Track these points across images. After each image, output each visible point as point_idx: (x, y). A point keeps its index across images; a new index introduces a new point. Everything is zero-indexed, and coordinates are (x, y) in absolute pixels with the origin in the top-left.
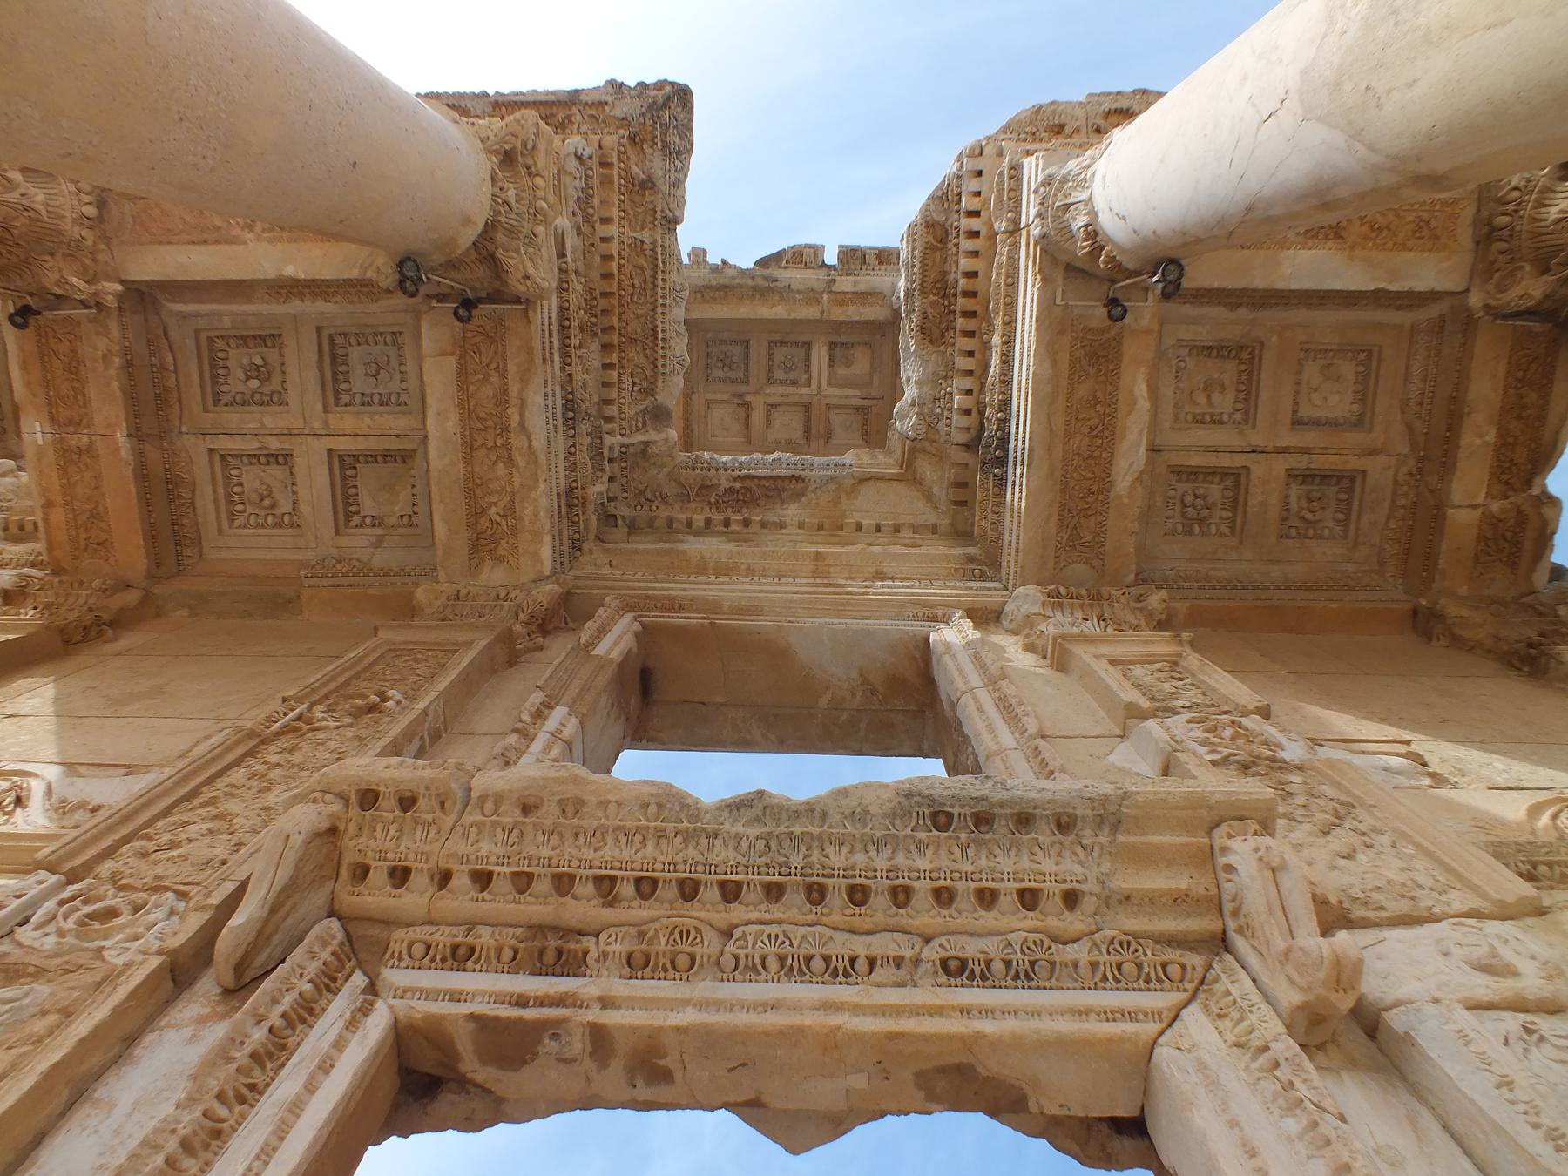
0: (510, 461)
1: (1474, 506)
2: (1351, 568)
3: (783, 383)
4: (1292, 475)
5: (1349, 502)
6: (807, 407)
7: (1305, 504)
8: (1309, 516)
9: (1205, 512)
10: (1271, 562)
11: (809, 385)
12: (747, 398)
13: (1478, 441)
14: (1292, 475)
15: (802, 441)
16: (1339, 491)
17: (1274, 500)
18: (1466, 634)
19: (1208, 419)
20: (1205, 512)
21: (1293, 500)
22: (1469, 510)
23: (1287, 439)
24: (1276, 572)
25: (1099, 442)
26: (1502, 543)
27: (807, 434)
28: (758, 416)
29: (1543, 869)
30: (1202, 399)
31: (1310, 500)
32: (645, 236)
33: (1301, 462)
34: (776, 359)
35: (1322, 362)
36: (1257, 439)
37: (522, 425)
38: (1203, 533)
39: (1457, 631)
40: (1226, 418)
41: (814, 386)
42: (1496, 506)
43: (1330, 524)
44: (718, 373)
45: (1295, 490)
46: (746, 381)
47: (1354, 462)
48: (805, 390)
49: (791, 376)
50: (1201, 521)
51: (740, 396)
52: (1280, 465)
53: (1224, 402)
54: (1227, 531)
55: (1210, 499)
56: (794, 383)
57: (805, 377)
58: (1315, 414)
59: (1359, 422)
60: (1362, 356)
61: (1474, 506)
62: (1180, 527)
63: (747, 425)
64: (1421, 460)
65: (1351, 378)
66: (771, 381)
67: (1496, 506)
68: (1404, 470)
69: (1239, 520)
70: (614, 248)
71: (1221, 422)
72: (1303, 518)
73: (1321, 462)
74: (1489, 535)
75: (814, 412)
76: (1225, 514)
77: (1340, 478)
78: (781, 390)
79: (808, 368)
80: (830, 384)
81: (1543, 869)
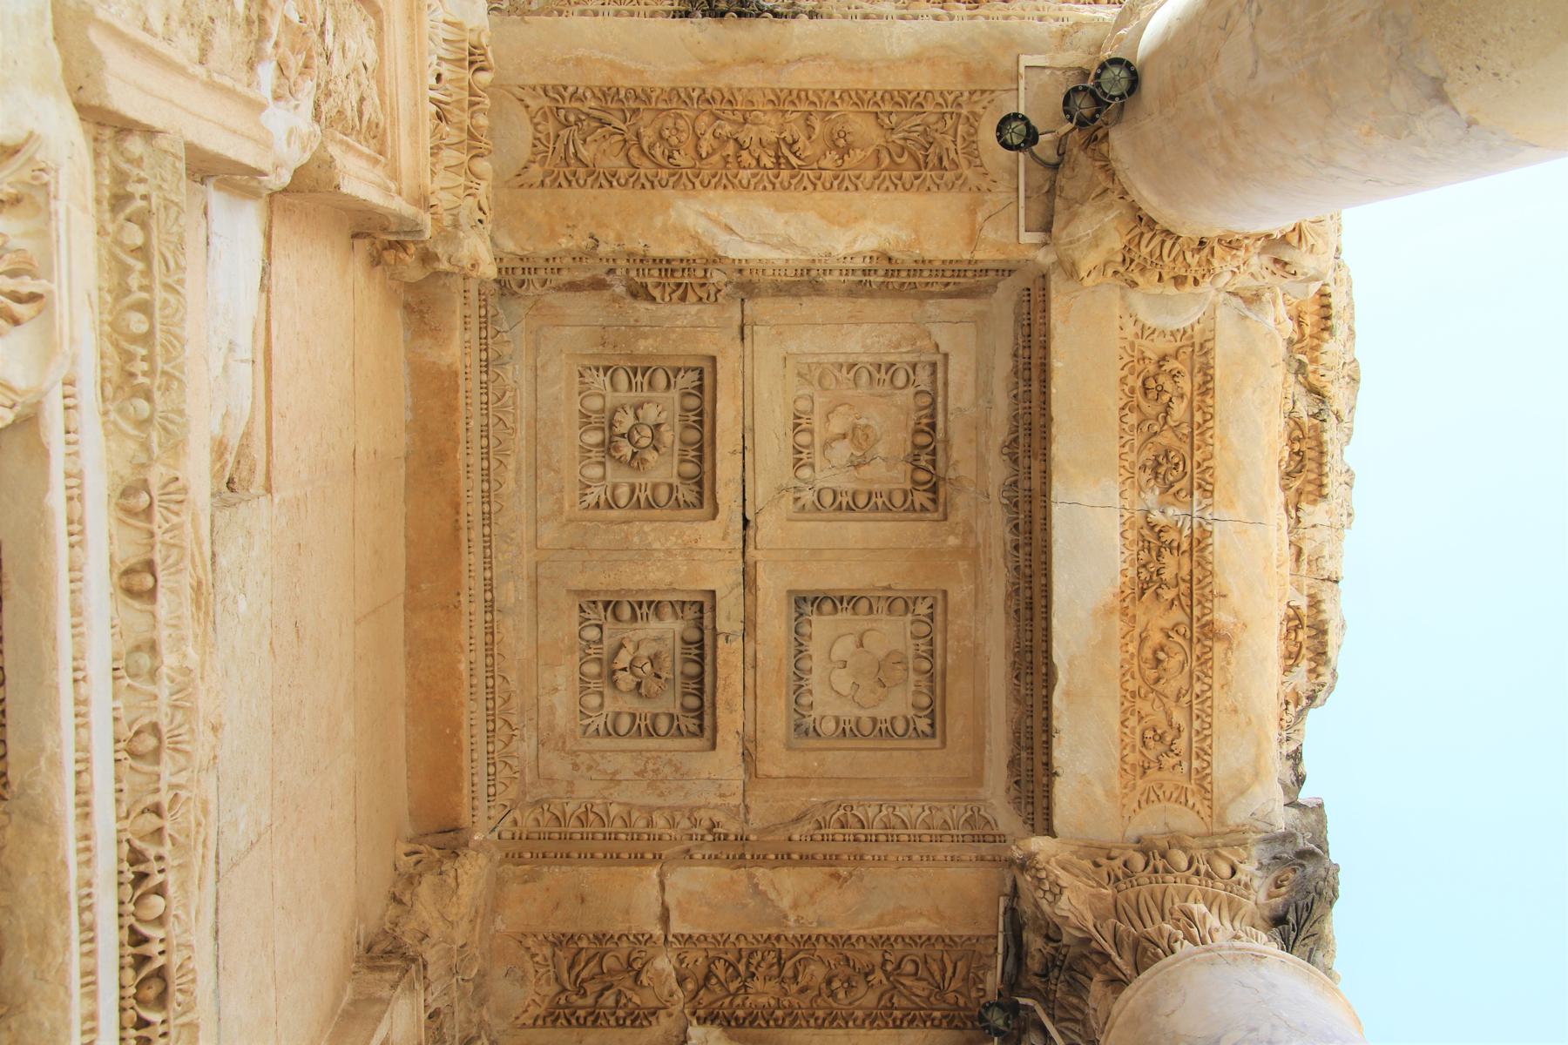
1: (665, 918)
2: (526, 747)
4: (702, 608)
5: (652, 732)
7: (644, 652)
8: (624, 659)
9: (626, 450)
10: (536, 583)
13: (785, 904)
14: (702, 608)
16: (671, 716)
17: (652, 577)
18: (424, 890)
19: (804, 439)
20: (626, 450)
21: (653, 627)
22: (658, 909)
23: (772, 587)
24: (512, 593)
25: (767, 161)
26: (592, 988)
29: (135, 236)
30: (837, 426)
31: (654, 659)
33: (728, 619)
35: (911, 654)
36: (768, 527)
38: (585, 450)
39: (429, 879)
40: (805, 473)
42: (664, 963)
43: (610, 707)
45: (670, 628)
47: (730, 721)
50: (608, 447)
52: (722, 578)
53: (832, 472)
54: (591, 499)
55: (651, 456)
58: (815, 648)
59: (803, 730)
60: (923, 724)
61: (665, 918)
62: (596, 403)
64: (742, 839)
65: (883, 712)
67: (664, 963)
68: (719, 817)
69: (615, 513)
71: (798, 464)
72: (621, 646)
73: (729, 655)
74: (609, 962)
76: (623, 493)
77: (699, 712)
81: (135, 236)
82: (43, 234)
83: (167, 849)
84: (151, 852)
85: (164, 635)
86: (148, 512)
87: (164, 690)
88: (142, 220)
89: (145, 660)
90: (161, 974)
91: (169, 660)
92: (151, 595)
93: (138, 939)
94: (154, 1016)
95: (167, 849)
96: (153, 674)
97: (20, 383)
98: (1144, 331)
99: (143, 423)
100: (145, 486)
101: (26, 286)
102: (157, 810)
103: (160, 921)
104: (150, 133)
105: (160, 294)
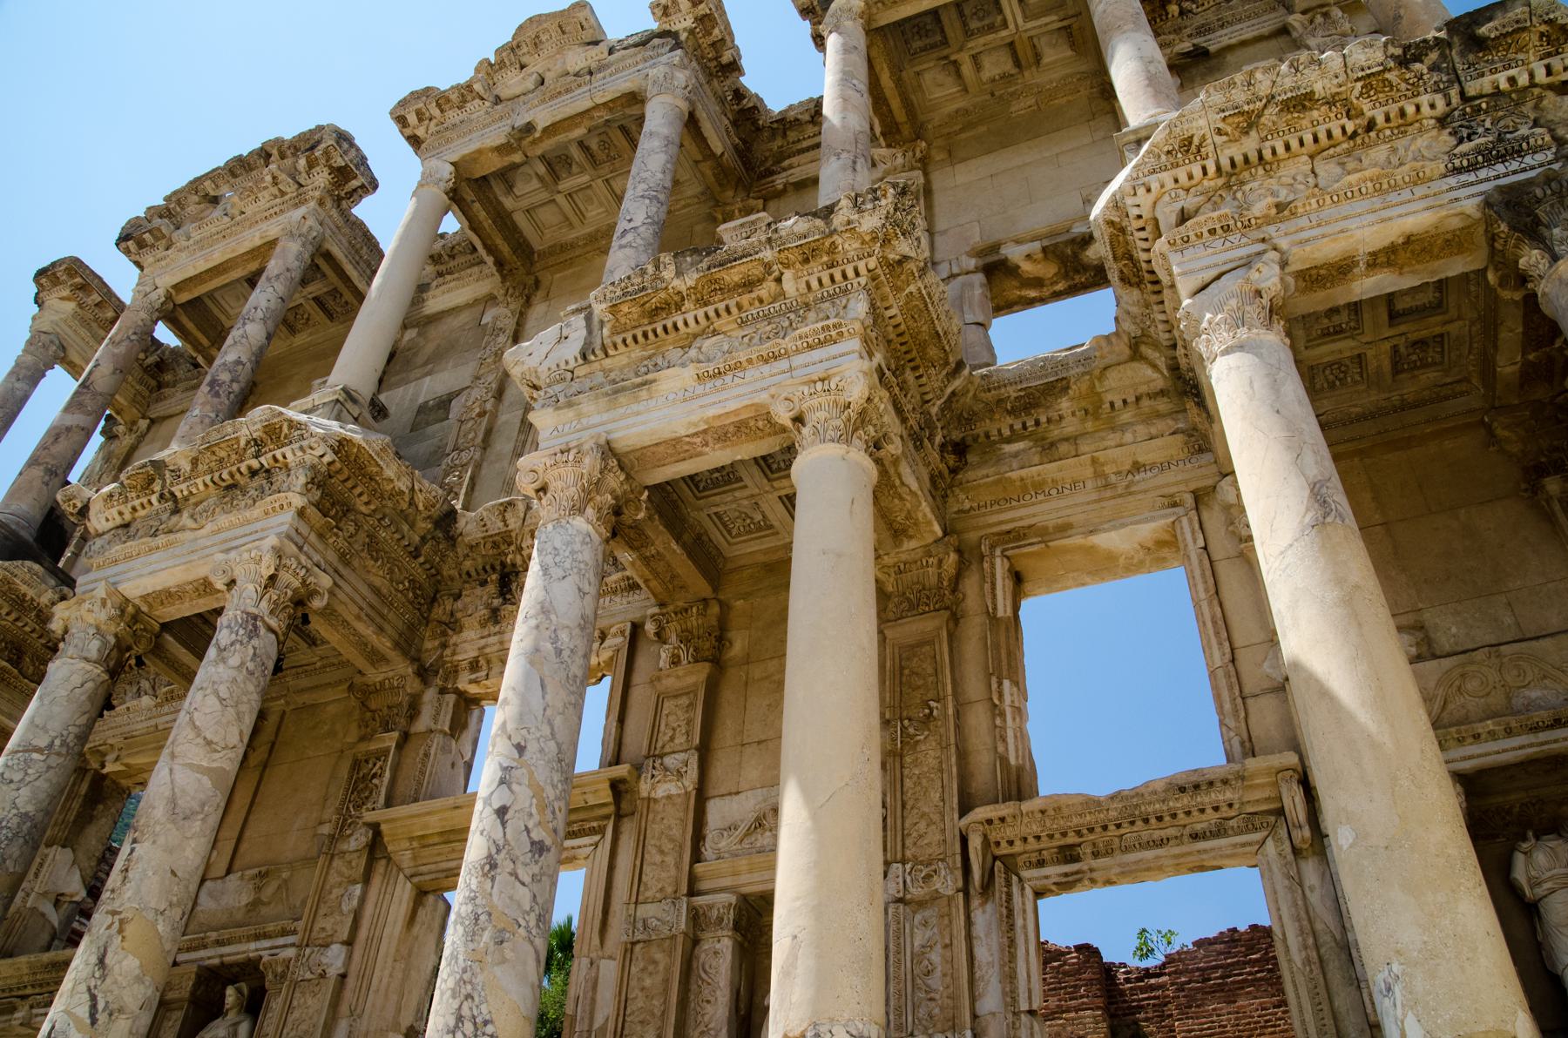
0: (901, 499)
3: (983, 31)
6: (1011, 45)
11: (1005, 25)
12: (953, 58)
15: (1014, 71)
27: (1017, 63)
28: (967, 69)
32: (912, 288)
34: (967, 12)
37: (903, 484)
41: (1012, 26)
44: (917, 44)
46: (945, 42)
48: (1004, 33)
49: (986, 22)
51: (946, 57)
56: (991, 28)
57: (999, 18)
63: (959, 75)
66: (969, 34)
70: (899, 319)
75: (1019, 47)
78: (982, 40)
79: (1000, 11)
80: (1026, 18)
98: (1297, 289)
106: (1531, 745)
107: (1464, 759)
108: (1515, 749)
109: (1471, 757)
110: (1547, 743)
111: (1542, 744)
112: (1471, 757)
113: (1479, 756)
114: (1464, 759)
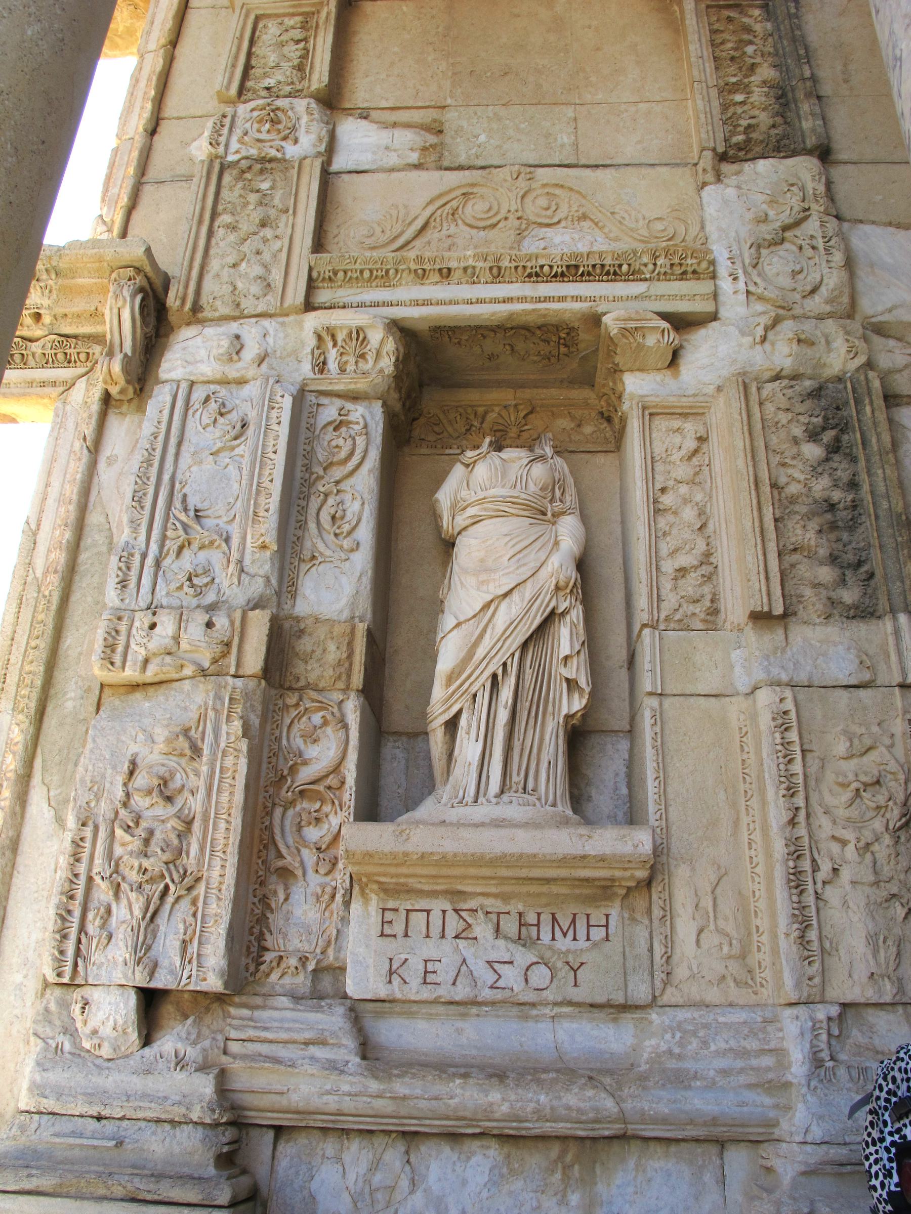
81: (341, 275)
82: (341, 328)
83: (529, 264)
84: (529, 271)
85: (462, 265)
86: (424, 270)
87: (480, 264)
88: (335, 273)
89: (469, 271)
90: (568, 267)
91: (471, 262)
92: (449, 269)
93: (555, 276)
94: (581, 270)
95: (529, 264)
96: (474, 268)
97: (381, 335)
99: (397, 271)
100: (416, 271)
101: (354, 335)
102: (516, 268)
103: (551, 267)
104: (311, 269)
105: (358, 266)
106: (522, 299)
107: (417, 303)
108: (495, 301)
109: (426, 303)
110: (547, 299)
111: (539, 300)
112: (426, 303)
113: (440, 303)
114: (417, 303)
